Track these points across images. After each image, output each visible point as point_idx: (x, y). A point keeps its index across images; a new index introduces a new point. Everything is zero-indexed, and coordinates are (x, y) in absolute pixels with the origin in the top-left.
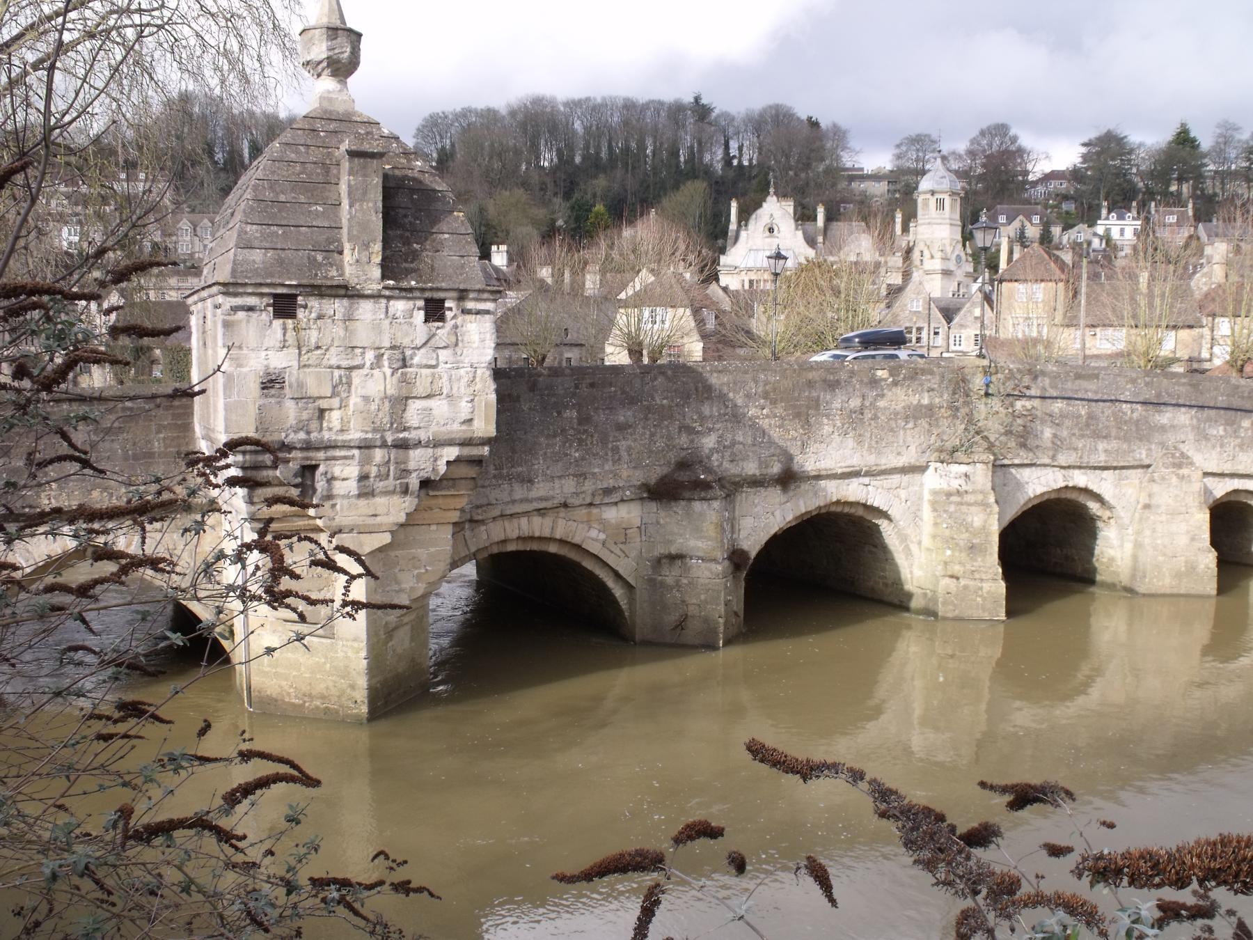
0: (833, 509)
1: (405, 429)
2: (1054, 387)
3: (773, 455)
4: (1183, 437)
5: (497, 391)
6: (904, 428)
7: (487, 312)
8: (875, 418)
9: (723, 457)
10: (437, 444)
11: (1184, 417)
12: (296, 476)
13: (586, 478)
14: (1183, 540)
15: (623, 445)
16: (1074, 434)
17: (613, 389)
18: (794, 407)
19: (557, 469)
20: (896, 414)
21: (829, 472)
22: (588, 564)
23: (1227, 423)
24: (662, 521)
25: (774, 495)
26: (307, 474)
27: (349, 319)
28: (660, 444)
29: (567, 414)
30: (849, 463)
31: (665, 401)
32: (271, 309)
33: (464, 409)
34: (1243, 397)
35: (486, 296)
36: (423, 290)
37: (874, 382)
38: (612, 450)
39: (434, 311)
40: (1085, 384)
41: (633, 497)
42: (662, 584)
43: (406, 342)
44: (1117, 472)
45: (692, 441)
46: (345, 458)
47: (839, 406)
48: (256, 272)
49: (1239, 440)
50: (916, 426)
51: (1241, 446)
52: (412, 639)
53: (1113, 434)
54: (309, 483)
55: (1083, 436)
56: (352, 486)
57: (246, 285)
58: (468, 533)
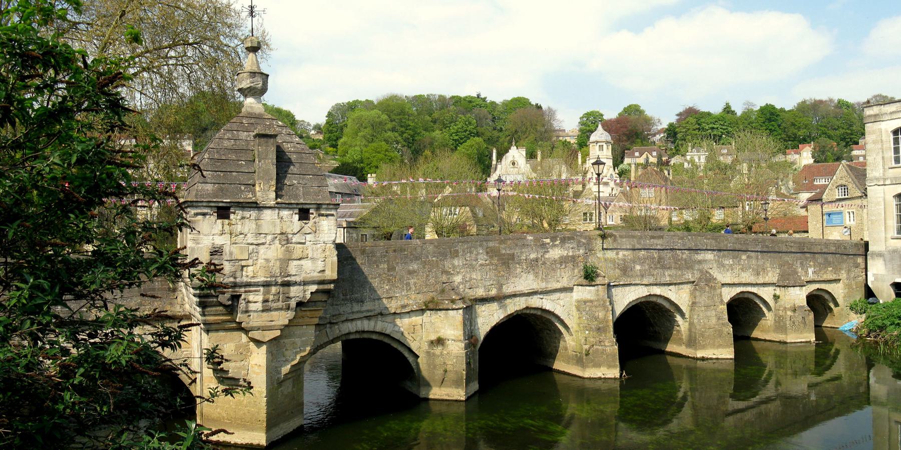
0: (525, 311)
1: (289, 276)
2: (640, 244)
3: (492, 285)
4: (711, 266)
5: (338, 255)
6: (559, 268)
7: (332, 215)
8: (544, 263)
9: (465, 286)
10: (305, 283)
11: (709, 256)
12: (228, 300)
13: (392, 299)
14: (714, 320)
15: (412, 281)
16: (651, 267)
17: (406, 253)
18: (503, 259)
20: (555, 261)
21: (521, 293)
22: (395, 345)
23: (733, 258)
24: (433, 321)
25: (495, 306)
26: (235, 300)
27: (258, 219)
28: (432, 281)
29: (382, 266)
30: (531, 287)
31: (434, 259)
32: (216, 214)
33: (320, 265)
34: (741, 244)
35: (331, 206)
36: (297, 204)
37: (543, 245)
38: (406, 284)
39: (304, 214)
40: (656, 241)
41: (418, 309)
42: (434, 354)
43: (289, 231)
44: (677, 286)
45: (449, 279)
46: (255, 291)
47: (524, 258)
48: (208, 195)
49: (741, 266)
50: (566, 267)
51: (742, 269)
52: (294, 386)
53: (673, 265)
54: (236, 304)
55: (656, 268)
56: (259, 306)
57: (202, 202)
58: (328, 330)
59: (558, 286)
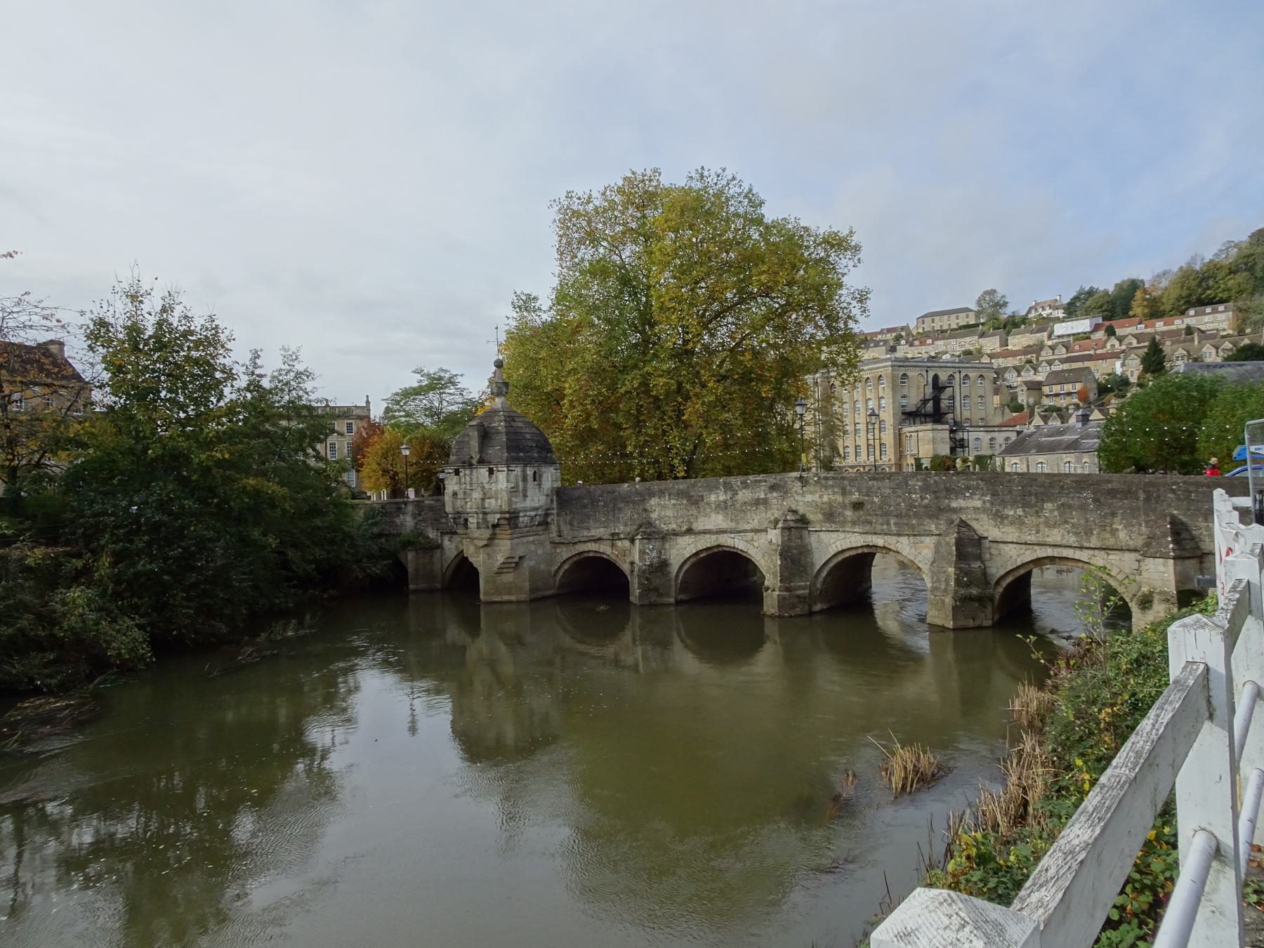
19: (597, 525)
20: (745, 503)
25: (687, 539)
59: (748, 527)
